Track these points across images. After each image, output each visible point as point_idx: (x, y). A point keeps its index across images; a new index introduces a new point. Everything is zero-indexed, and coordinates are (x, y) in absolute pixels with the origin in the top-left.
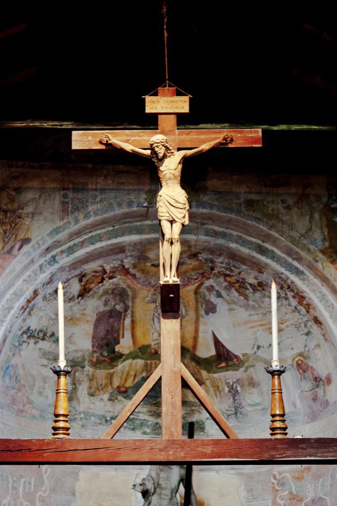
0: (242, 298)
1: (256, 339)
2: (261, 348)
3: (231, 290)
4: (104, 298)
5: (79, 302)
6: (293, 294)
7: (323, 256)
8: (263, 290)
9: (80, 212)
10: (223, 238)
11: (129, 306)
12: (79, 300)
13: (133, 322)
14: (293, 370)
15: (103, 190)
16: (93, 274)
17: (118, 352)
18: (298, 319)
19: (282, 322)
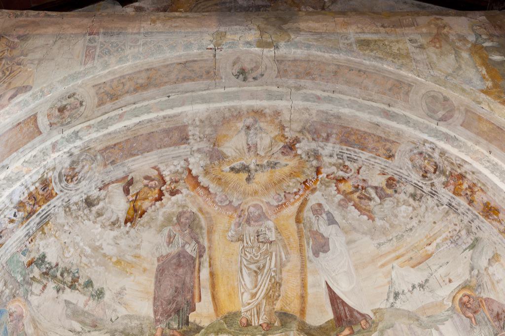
0: (365, 217)
1: (391, 283)
2: (401, 296)
3: (347, 208)
4: (166, 231)
5: (128, 232)
6: (443, 179)
7: (488, 97)
8: (396, 191)
9: (112, 56)
10: (329, 103)
11: (204, 248)
12: (127, 229)
13: (212, 275)
14: (455, 316)
15: (146, 34)
16: (146, 182)
17: (194, 324)
18: (456, 225)
19: (429, 242)
